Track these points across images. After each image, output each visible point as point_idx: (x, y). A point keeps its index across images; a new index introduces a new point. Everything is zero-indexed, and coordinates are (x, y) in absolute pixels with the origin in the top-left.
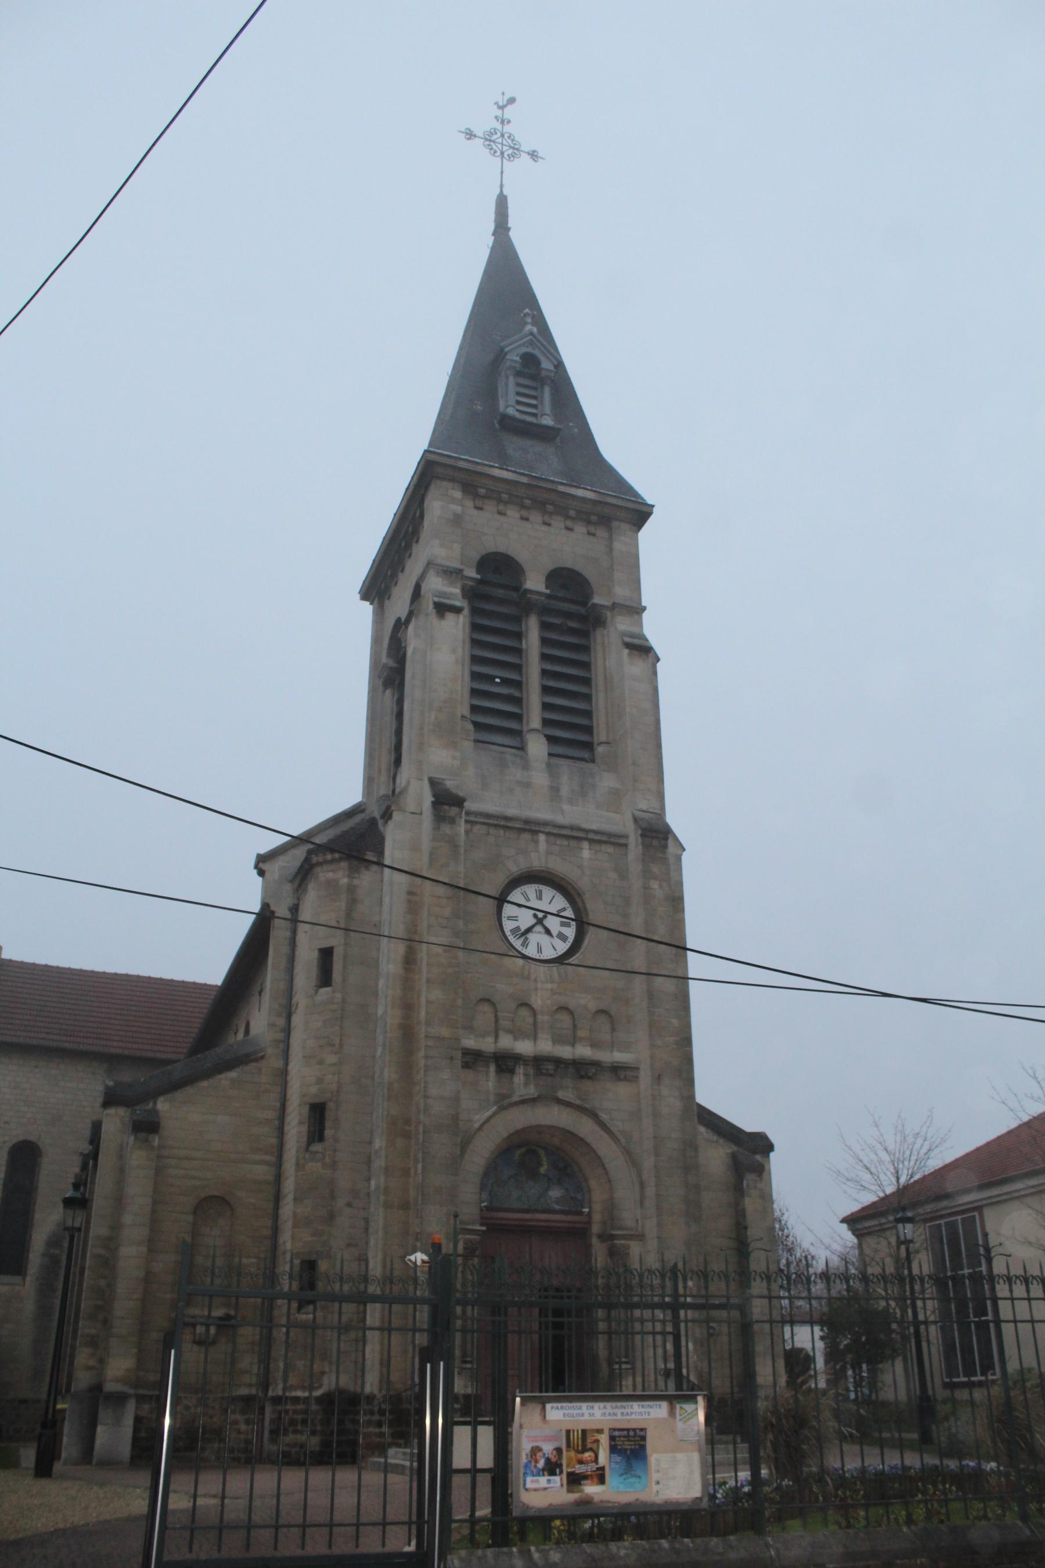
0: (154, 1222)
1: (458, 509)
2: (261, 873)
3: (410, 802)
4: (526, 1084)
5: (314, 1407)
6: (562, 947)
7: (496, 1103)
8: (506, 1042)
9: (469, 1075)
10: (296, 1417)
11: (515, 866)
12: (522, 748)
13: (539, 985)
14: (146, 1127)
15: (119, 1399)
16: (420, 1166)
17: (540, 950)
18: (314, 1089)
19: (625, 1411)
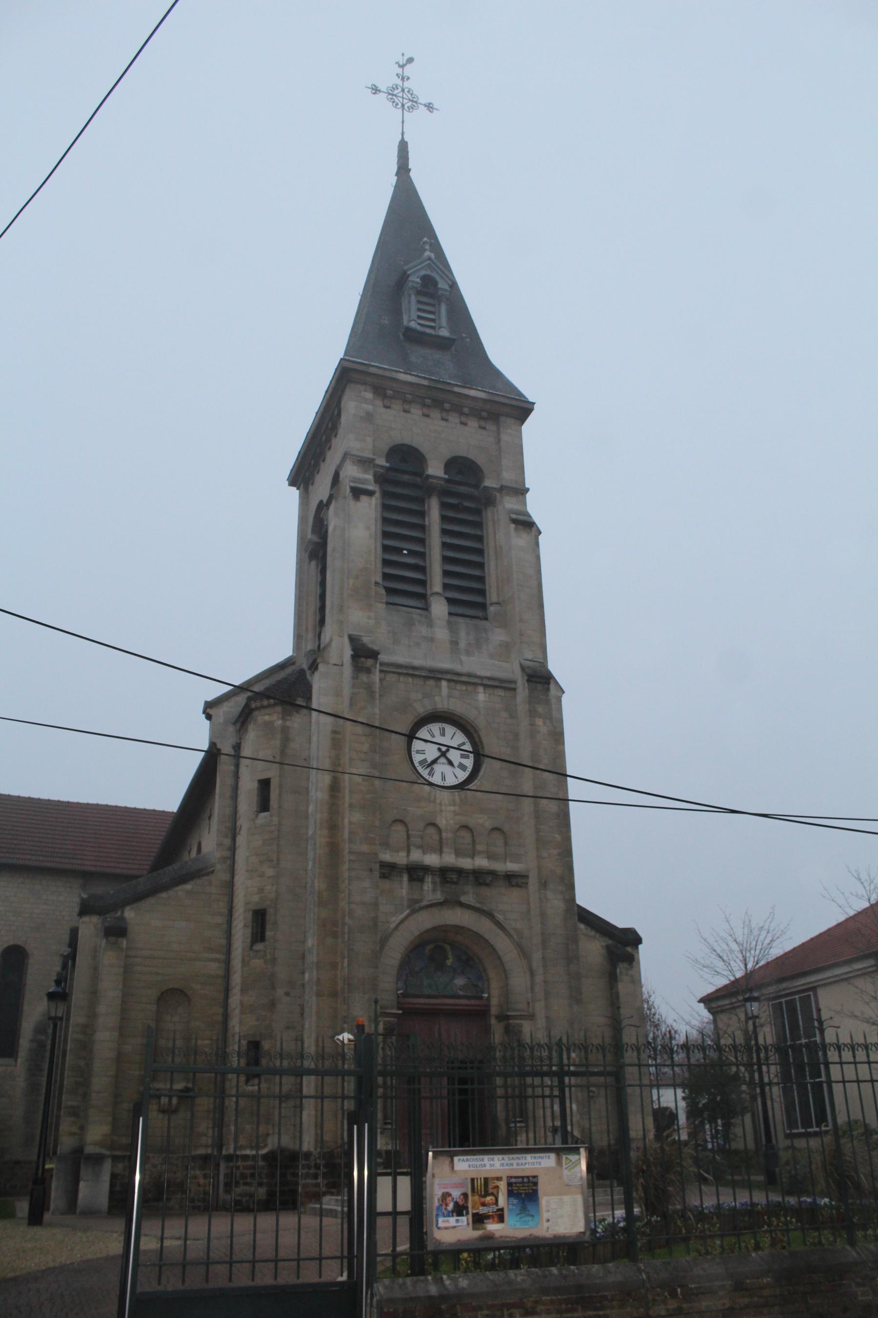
0: (124, 1014)
1: (370, 408)
2: (209, 717)
3: (333, 655)
4: (434, 890)
5: (261, 1163)
6: (463, 776)
7: (409, 907)
8: (416, 856)
9: (386, 884)
10: (245, 1171)
11: (422, 708)
12: (426, 609)
13: (443, 808)
14: (116, 931)
15: (97, 1160)
16: (346, 960)
17: (444, 778)
18: (256, 898)
19: (520, 1162)
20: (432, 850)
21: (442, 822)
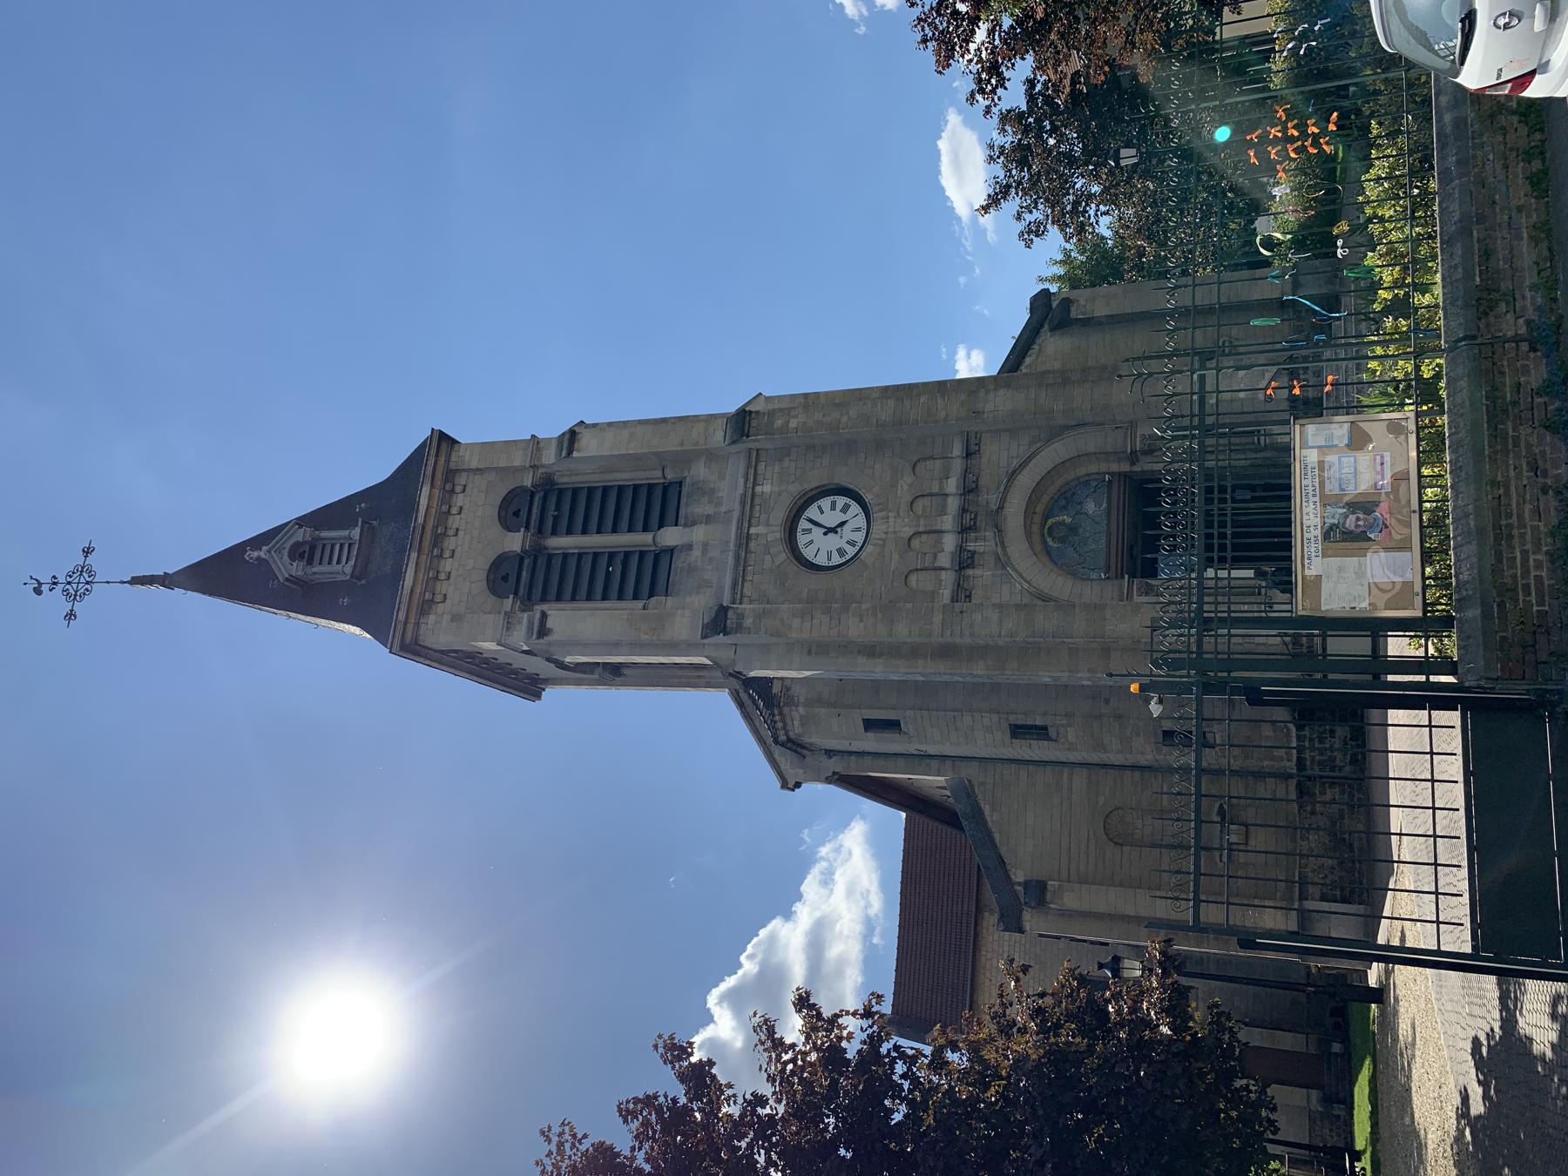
1: (447, 618)
2: (798, 785)
3: (725, 655)
4: (984, 539)
5: (1307, 732)
6: (855, 508)
7: (1004, 567)
8: (944, 560)
11: (783, 556)
12: (671, 551)
14: (1038, 891)
17: (858, 530)
20: (939, 542)
21: (907, 531)
